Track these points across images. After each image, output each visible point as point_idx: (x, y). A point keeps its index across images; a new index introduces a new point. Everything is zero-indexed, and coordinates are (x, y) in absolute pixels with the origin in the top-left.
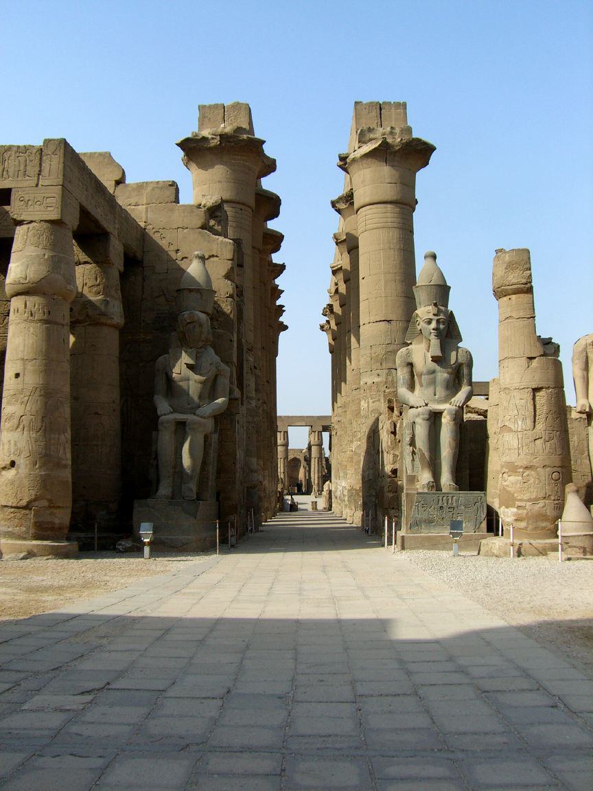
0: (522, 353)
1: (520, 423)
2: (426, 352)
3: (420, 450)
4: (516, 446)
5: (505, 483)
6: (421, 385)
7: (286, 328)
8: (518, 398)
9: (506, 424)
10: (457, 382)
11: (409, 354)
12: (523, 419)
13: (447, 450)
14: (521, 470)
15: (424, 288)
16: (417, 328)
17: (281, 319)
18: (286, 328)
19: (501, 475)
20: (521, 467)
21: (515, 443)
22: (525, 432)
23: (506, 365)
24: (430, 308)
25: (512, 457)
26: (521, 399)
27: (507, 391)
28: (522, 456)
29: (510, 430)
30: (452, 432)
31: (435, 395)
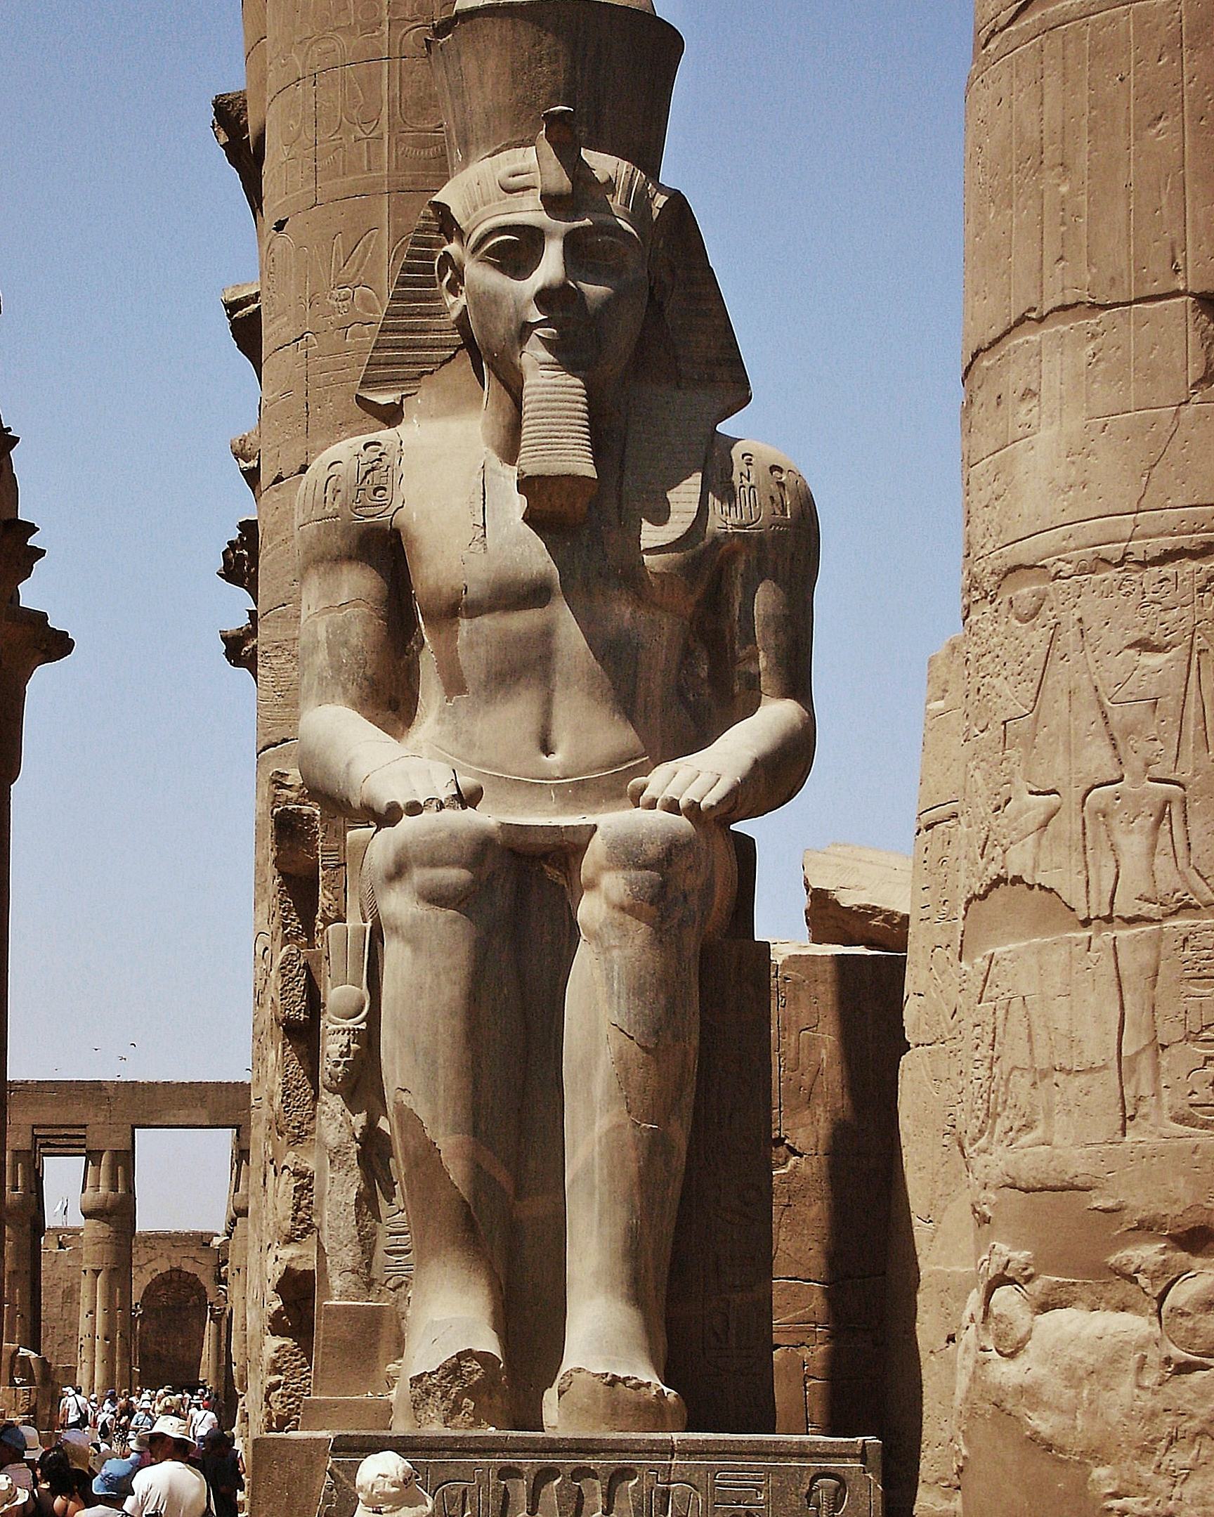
0: (1159, 266)
1: (1133, 844)
2: (495, 461)
3: (407, 1118)
4: (1096, 1044)
5: (1006, 1373)
6: (454, 685)
7: (59, 645)
8: (1115, 638)
9: (1018, 861)
10: (704, 671)
11: (376, 476)
12: (1162, 815)
13: (602, 1124)
14: (1147, 1253)
15: (494, 29)
16: (442, 312)
17: (30, 595)
18: (59, 645)
19: (976, 1297)
20: (1146, 1228)
21: (1089, 1022)
22: (1182, 922)
23: (1015, 378)
24: (526, 158)
25: (1064, 1142)
26: (1144, 645)
27: (1025, 592)
28: (1156, 1130)
29: (1051, 907)
30: (638, 991)
31: (546, 748)
